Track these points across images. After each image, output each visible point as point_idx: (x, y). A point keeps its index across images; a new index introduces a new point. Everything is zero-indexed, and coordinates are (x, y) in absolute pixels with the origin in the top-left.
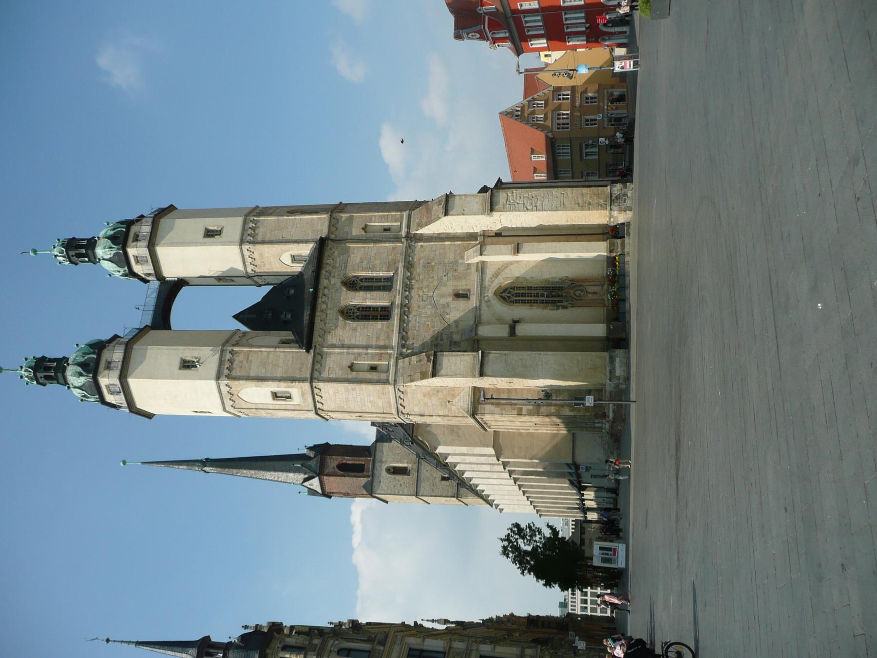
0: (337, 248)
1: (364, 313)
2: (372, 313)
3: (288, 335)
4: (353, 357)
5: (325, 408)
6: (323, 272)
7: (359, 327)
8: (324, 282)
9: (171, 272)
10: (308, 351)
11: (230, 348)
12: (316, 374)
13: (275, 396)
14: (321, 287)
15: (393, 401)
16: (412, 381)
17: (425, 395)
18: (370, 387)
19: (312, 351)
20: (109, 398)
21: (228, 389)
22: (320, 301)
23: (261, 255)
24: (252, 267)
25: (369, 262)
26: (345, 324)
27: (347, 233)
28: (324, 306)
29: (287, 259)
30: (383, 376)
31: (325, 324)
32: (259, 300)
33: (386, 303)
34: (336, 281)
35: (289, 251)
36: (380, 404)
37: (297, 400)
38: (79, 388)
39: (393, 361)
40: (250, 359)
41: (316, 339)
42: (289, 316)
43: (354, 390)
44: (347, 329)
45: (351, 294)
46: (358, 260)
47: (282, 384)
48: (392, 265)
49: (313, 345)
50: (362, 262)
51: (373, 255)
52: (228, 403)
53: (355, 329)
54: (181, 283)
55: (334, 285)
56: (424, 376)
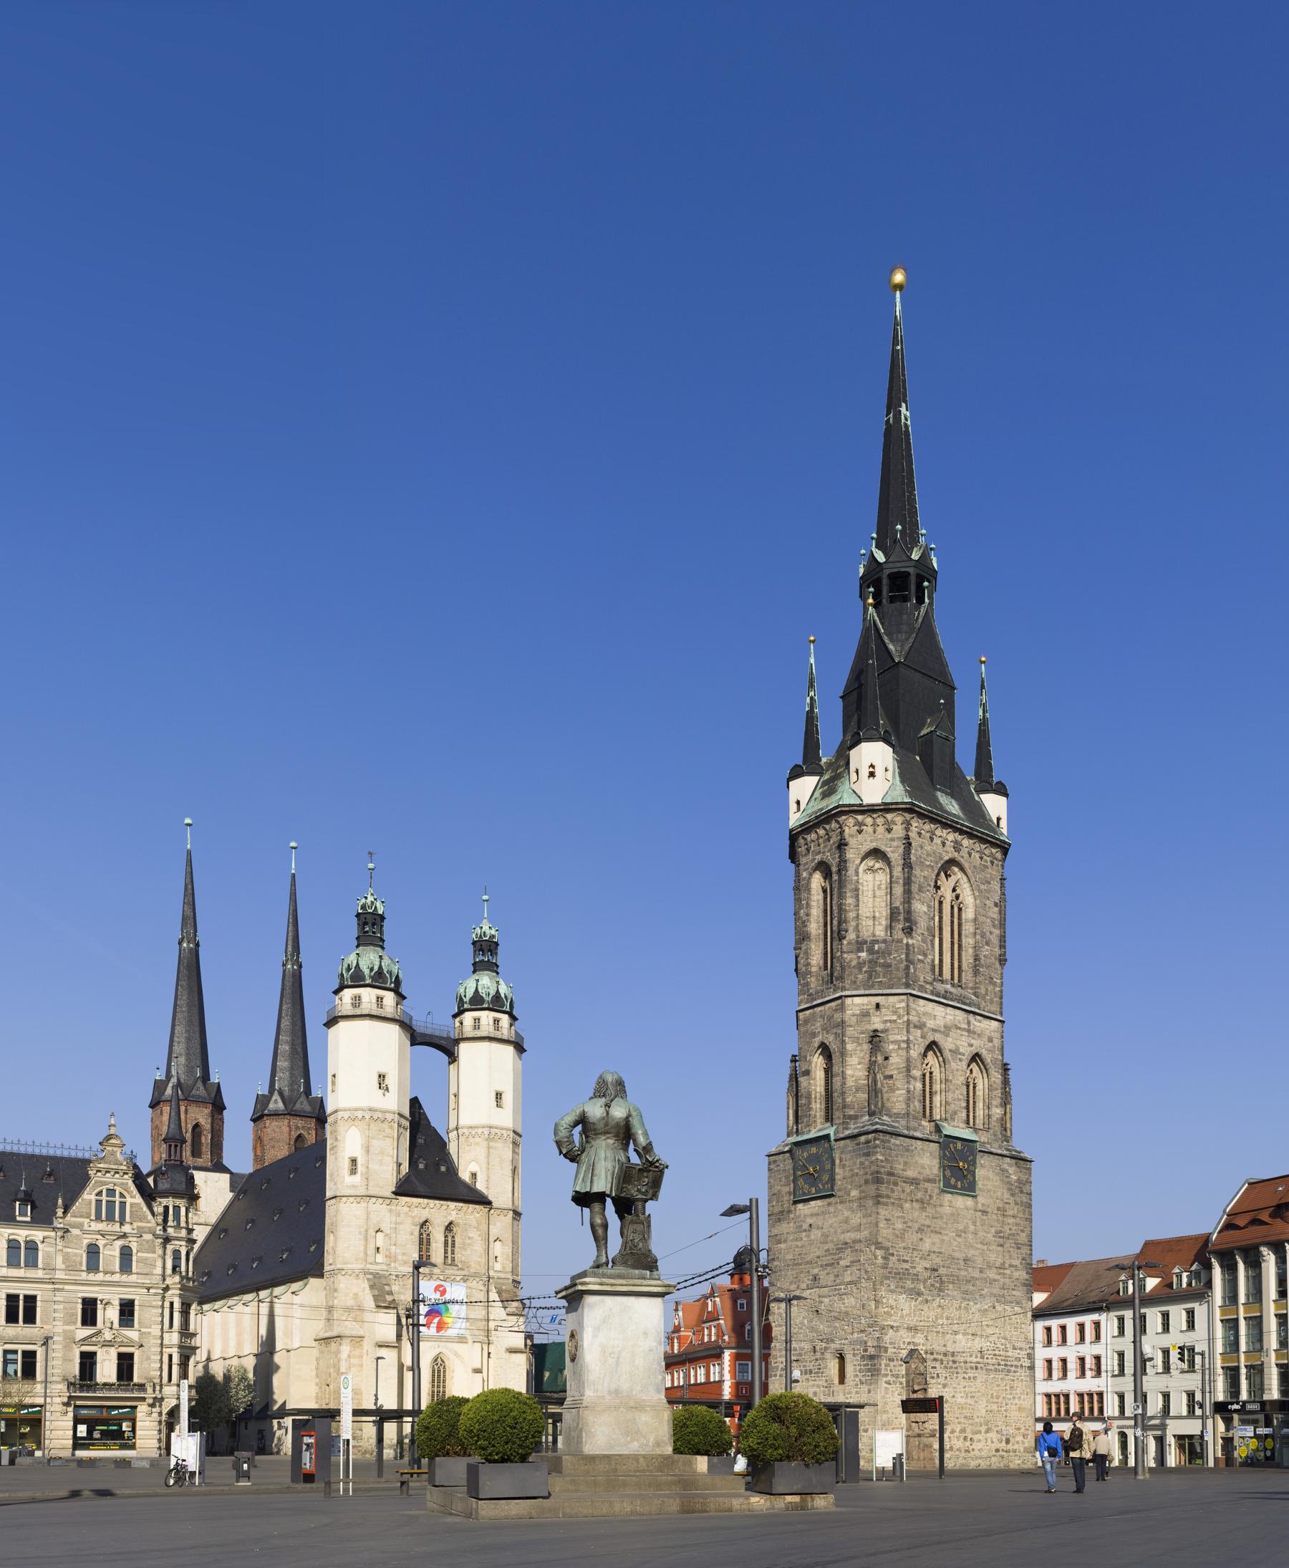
0: (482, 1216)
1: (425, 1241)
2: (424, 1248)
3: (405, 1168)
4: (388, 1232)
5: (342, 1205)
6: (461, 1204)
7: (413, 1237)
8: (452, 1205)
9: (464, 1049)
10: (393, 1193)
11: (396, 1120)
12: (374, 1200)
13: (354, 1161)
14: (449, 1203)
15: (349, 1266)
16: (372, 1287)
17: (356, 1294)
18: (362, 1248)
19: (394, 1196)
20: (348, 994)
21: (360, 1117)
22: (437, 1202)
23: (477, 1144)
24: (467, 1133)
25: (469, 1244)
26: (416, 1225)
27: (495, 1225)
28: (432, 1206)
29: (474, 1167)
30: (371, 1259)
31: (417, 1207)
32: (433, 1124)
33: (433, 1260)
34: (453, 1216)
35: (481, 1171)
36: (346, 1255)
37: (350, 1180)
38: (358, 963)
39: (385, 1267)
40: (388, 1139)
41: (404, 1199)
42: (421, 1166)
43: (360, 1233)
44: (413, 1227)
45: (443, 1229)
46: (471, 1235)
47: (364, 1170)
48: (467, 1265)
49: (398, 1197)
50: (469, 1238)
51: (476, 1248)
52: (346, 1115)
53: (412, 1234)
54: (452, 1057)
55: (450, 1214)
56: (376, 1298)
